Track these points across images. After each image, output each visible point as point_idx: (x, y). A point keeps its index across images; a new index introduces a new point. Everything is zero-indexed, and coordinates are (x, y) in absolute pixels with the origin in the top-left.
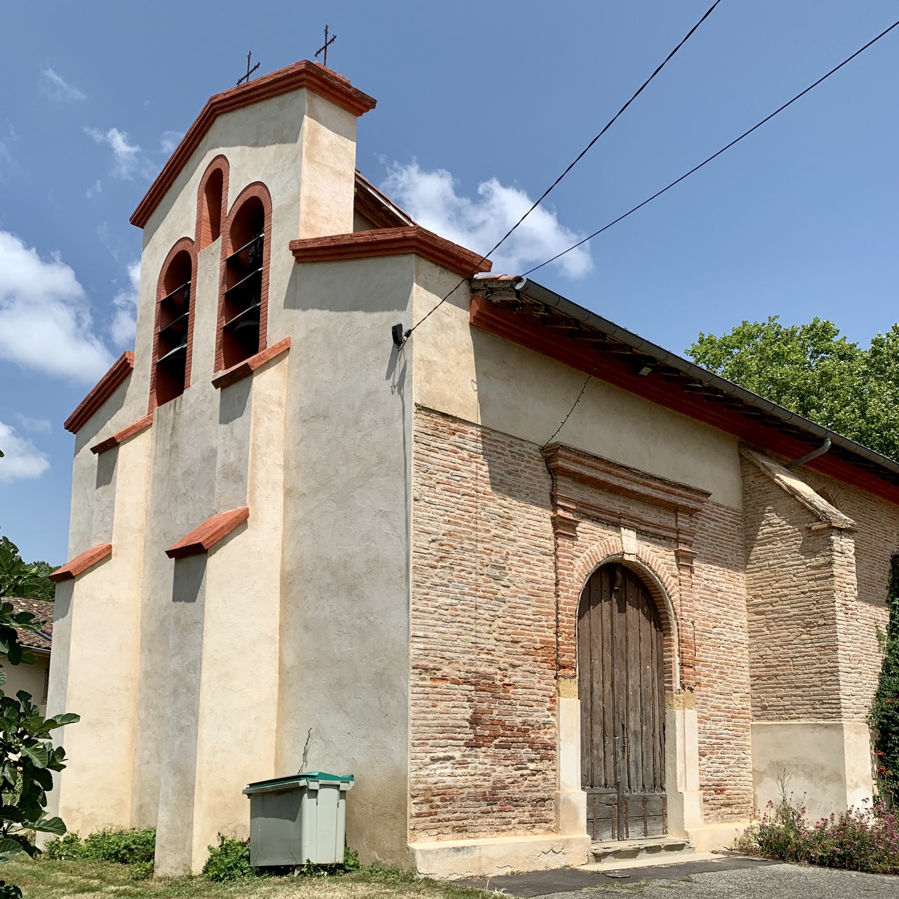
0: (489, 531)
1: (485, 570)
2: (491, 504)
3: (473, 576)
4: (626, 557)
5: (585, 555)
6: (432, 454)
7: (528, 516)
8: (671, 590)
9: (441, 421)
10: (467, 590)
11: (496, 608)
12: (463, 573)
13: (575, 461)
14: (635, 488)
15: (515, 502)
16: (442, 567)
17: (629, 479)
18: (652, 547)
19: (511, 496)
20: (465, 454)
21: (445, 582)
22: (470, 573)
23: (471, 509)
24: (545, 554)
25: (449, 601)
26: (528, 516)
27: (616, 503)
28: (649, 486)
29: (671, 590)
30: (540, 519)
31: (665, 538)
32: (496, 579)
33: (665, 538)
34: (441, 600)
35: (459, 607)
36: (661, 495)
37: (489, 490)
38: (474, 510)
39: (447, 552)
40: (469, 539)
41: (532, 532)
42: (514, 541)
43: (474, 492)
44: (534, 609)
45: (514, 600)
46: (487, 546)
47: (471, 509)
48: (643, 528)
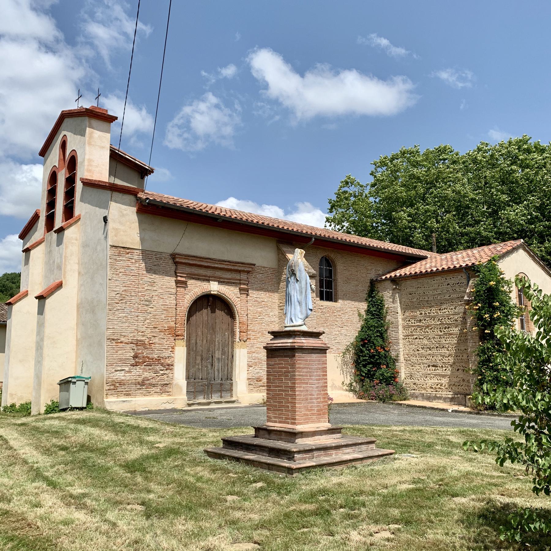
0: (144, 288)
1: (142, 303)
2: (145, 278)
3: (136, 305)
4: (212, 293)
5: (191, 293)
6: (118, 262)
7: (163, 281)
8: (236, 303)
9: (122, 250)
10: (133, 310)
11: (147, 316)
12: (131, 304)
13: (185, 259)
14: (216, 266)
15: (157, 276)
16: (121, 303)
17: (213, 263)
18: (227, 287)
19: (155, 274)
20: (133, 261)
21: (123, 308)
22: (135, 304)
23: (136, 281)
24: (171, 294)
25: (124, 315)
26: (163, 281)
27: (209, 272)
28: (224, 264)
29: (236, 303)
30: (169, 281)
31: (234, 283)
32: (147, 305)
33: (234, 283)
34: (121, 315)
35: (129, 317)
36: (230, 267)
37: (145, 272)
38: (138, 281)
39: (124, 297)
40: (134, 292)
41: (165, 287)
42: (156, 291)
43: (137, 274)
44: (165, 315)
45: (155, 312)
46: (143, 294)
47: (136, 281)
48: (221, 280)
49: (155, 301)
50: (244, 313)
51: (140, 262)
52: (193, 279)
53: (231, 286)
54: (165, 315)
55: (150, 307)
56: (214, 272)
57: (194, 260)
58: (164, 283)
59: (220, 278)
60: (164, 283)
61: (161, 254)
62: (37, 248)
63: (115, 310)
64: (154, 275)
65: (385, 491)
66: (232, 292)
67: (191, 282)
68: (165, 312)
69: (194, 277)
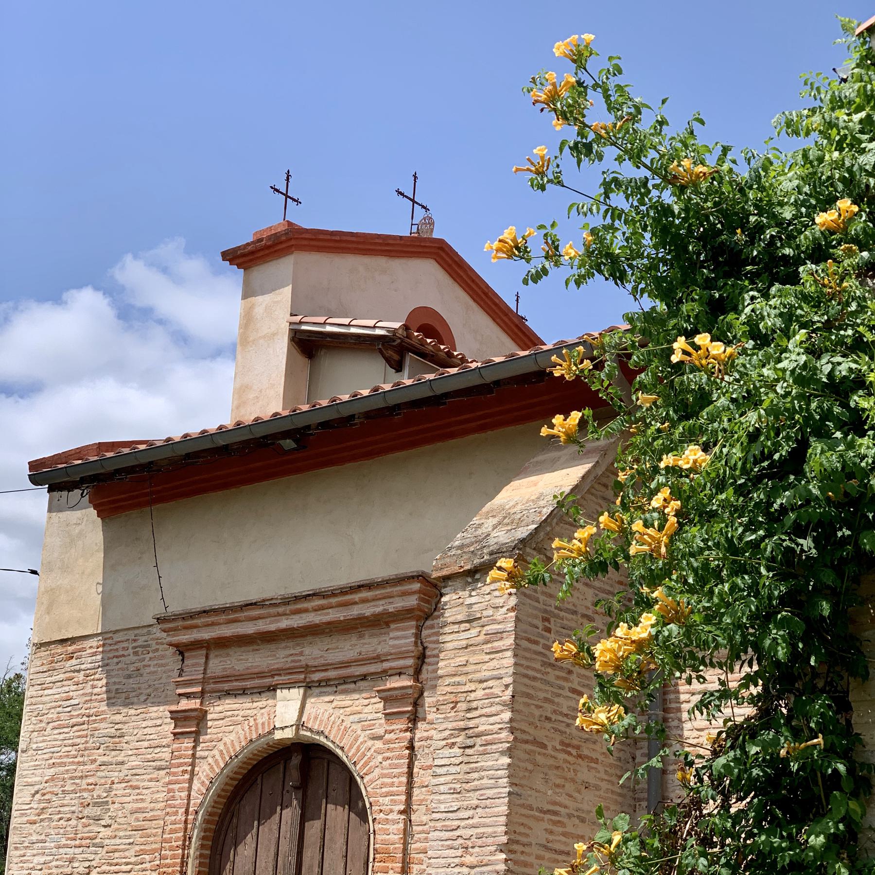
0: (95, 760)
1: (86, 812)
2: (103, 725)
3: (73, 822)
4: (278, 735)
5: (216, 752)
6: (46, 692)
7: (144, 724)
8: (366, 764)
10: (64, 841)
11: (92, 857)
12: (62, 822)
13: (186, 628)
14: (284, 623)
15: (132, 712)
16: (42, 820)
17: (270, 616)
18: (341, 700)
19: (126, 705)
20: (81, 676)
21: (43, 837)
22: (69, 820)
23: (78, 741)
24: (160, 769)
25: (42, 859)
26: (144, 724)
27: (282, 653)
28: (306, 611)
29: (366, 764)
30: (159, 722)
31: (364, 677)
32: (98, 819)
33: (364, 677)
34: (36, 860)
35: (54, 863)
36: (333, 615)
37: (103, 707)
38: (83, 740)
39: (49, 801)
40: (71, 778)
41: (146, 744)
42: (122, 763)
43: (85, 719)
44: (137, 848)
45: (113, 841)
46: (90, 780)
47: (78, 741)
48: (316, 677)
49: (117, 800)
50: (394, 802)
51: (97, 676)
52: (228, 694)
53: (354, 691)
54: (137, 848)
55: (103, 822)
56: (298, 650)
57: (213, 624)
58: (146, 731)
59: (307, 669)
60: (146, 731)
61: (149, 633)
62: (206, 448)
63: (26, 844)
64: (124, 710)
65: (68, 856)
66: (356, 718)
67: (218, 709)
68: (137, 837)
69: (226, 686)
